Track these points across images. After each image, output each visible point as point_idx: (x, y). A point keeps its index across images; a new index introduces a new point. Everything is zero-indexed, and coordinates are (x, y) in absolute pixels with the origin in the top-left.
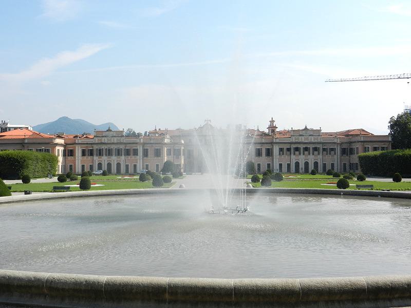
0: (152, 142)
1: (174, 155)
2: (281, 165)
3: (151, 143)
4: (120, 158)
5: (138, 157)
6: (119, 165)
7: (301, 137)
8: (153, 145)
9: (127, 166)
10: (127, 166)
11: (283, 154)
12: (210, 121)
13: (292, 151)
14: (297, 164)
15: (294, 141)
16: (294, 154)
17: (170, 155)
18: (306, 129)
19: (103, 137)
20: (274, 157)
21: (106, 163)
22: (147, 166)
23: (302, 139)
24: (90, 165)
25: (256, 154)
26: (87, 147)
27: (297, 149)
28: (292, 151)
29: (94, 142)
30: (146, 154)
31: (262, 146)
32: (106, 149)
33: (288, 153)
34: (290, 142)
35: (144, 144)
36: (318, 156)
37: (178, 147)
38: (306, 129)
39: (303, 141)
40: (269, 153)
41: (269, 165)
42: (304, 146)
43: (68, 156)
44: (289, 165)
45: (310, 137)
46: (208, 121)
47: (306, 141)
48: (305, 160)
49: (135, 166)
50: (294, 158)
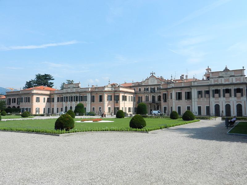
0: (97, 90)
1: (115, 100)
2: (199, 108)
3: (96, 92)
5: (87, 102)
7: (220, 79)
8: (98, 93)
11: (202, 97)
12: (154, 73)
13: (211, 93)
14: (217, 107)
15: (213, 83)
17: (111, 100)
18: (226, 70)
20: (193, 100)
22: (94, 108)
23: (222, 81)
24: (61, 108)
25: (176, 98)
26: (60, 95)
27: (217, 91)
28: (211, 93)
30: (93, 100)
31: (181, 90)
32: (70, 97)
33: (207, 95)
34: (208, 84)
35: (91, 92)
36: (242, 98)
37: (117, 94)
38: (226, 70)
39: (223, 82)
40: (189, 96)
41: (189, 108)
42: (225, 88)
43: (52, 102)
44: (208, 108)
45: (231, 78)
46: (152, 73)
47: (227, 83)
48: (226, 102)
50: (213, 101)
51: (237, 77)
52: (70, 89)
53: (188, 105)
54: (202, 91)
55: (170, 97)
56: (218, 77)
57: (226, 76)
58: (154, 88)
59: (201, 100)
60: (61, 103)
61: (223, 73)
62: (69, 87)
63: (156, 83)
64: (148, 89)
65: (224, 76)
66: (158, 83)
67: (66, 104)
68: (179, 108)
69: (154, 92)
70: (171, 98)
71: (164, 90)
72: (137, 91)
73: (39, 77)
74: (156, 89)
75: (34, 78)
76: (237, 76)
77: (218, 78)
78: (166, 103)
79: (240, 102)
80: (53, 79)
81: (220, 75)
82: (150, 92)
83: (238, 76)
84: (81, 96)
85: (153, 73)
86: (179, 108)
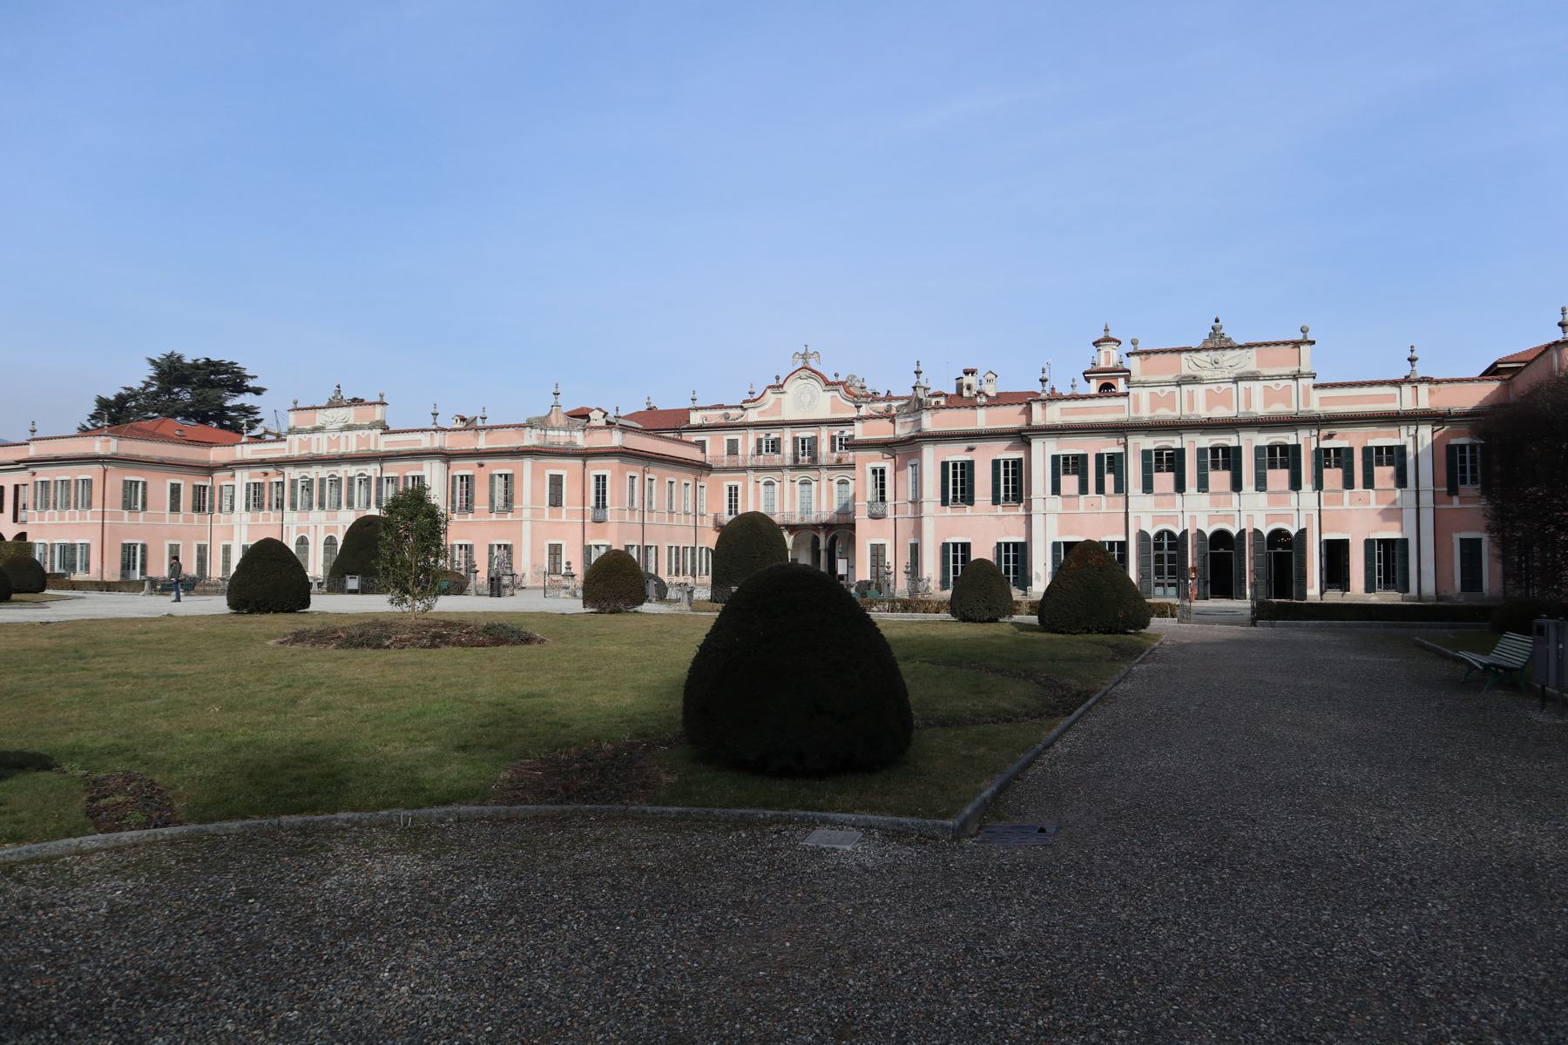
4: (336, 518)
15: (1145, 414)
16: (1148, 487)
20: (1037, 505)
21: (322, 539)
29: (286, 454)
31: (971, 449)
47: (1220, 413)
51: (1271, 384)
52: (323, 437)
54: (1085, 457)
56: (1170, 377)
57: (1218, 374)
59: (1082, 510)
60: (274, 515)
61: (1203, 355)
62: (318, 424)
63: (824, 405)
64: (775, 446)
65: (1204, 374)
66: (833, 410)
67: (304, 525)
69: (814, 459)
71: (877, 453)
72: (719, 453)
73: (172, 372)
74: (824, 447)
75: (137, 375)
76: (1271, 378)
77: (1168, 384)
78: (888, 523)
79: (1287, 522)
80: (258, 391)
81: (1186, 371)
82: (788, 462)
83: (1281, 377)
84: (384, 475)
85: (811, 351)
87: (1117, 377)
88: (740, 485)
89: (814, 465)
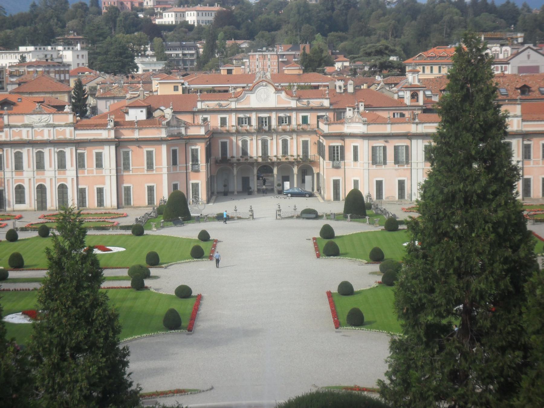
6: (62, 189)
9: (82, 193)
10: (82, 193)
19: (25, 126)
20: (414, 166)
31: (386, 142)
41: (401, 184)
49: (100, 191)
53: (400, 176)
55: (349, 154)
58: (270, 118)
68: (379, 184)
70: (356, 159)
74: (274, 123)
78: (341, 171)
86: (379, 184)
87: (419, 91)
88: (228, 141)
89: (270, 132)
